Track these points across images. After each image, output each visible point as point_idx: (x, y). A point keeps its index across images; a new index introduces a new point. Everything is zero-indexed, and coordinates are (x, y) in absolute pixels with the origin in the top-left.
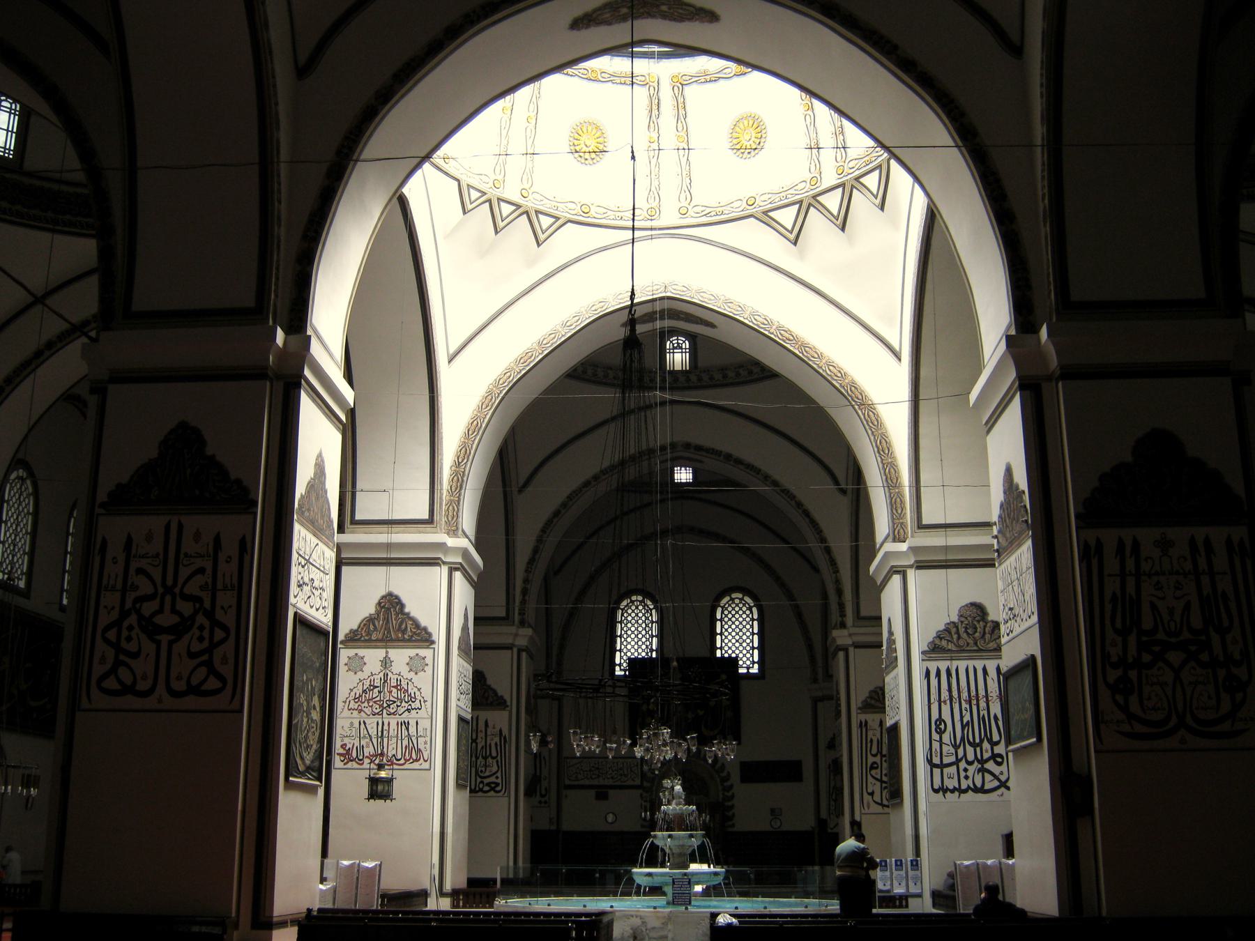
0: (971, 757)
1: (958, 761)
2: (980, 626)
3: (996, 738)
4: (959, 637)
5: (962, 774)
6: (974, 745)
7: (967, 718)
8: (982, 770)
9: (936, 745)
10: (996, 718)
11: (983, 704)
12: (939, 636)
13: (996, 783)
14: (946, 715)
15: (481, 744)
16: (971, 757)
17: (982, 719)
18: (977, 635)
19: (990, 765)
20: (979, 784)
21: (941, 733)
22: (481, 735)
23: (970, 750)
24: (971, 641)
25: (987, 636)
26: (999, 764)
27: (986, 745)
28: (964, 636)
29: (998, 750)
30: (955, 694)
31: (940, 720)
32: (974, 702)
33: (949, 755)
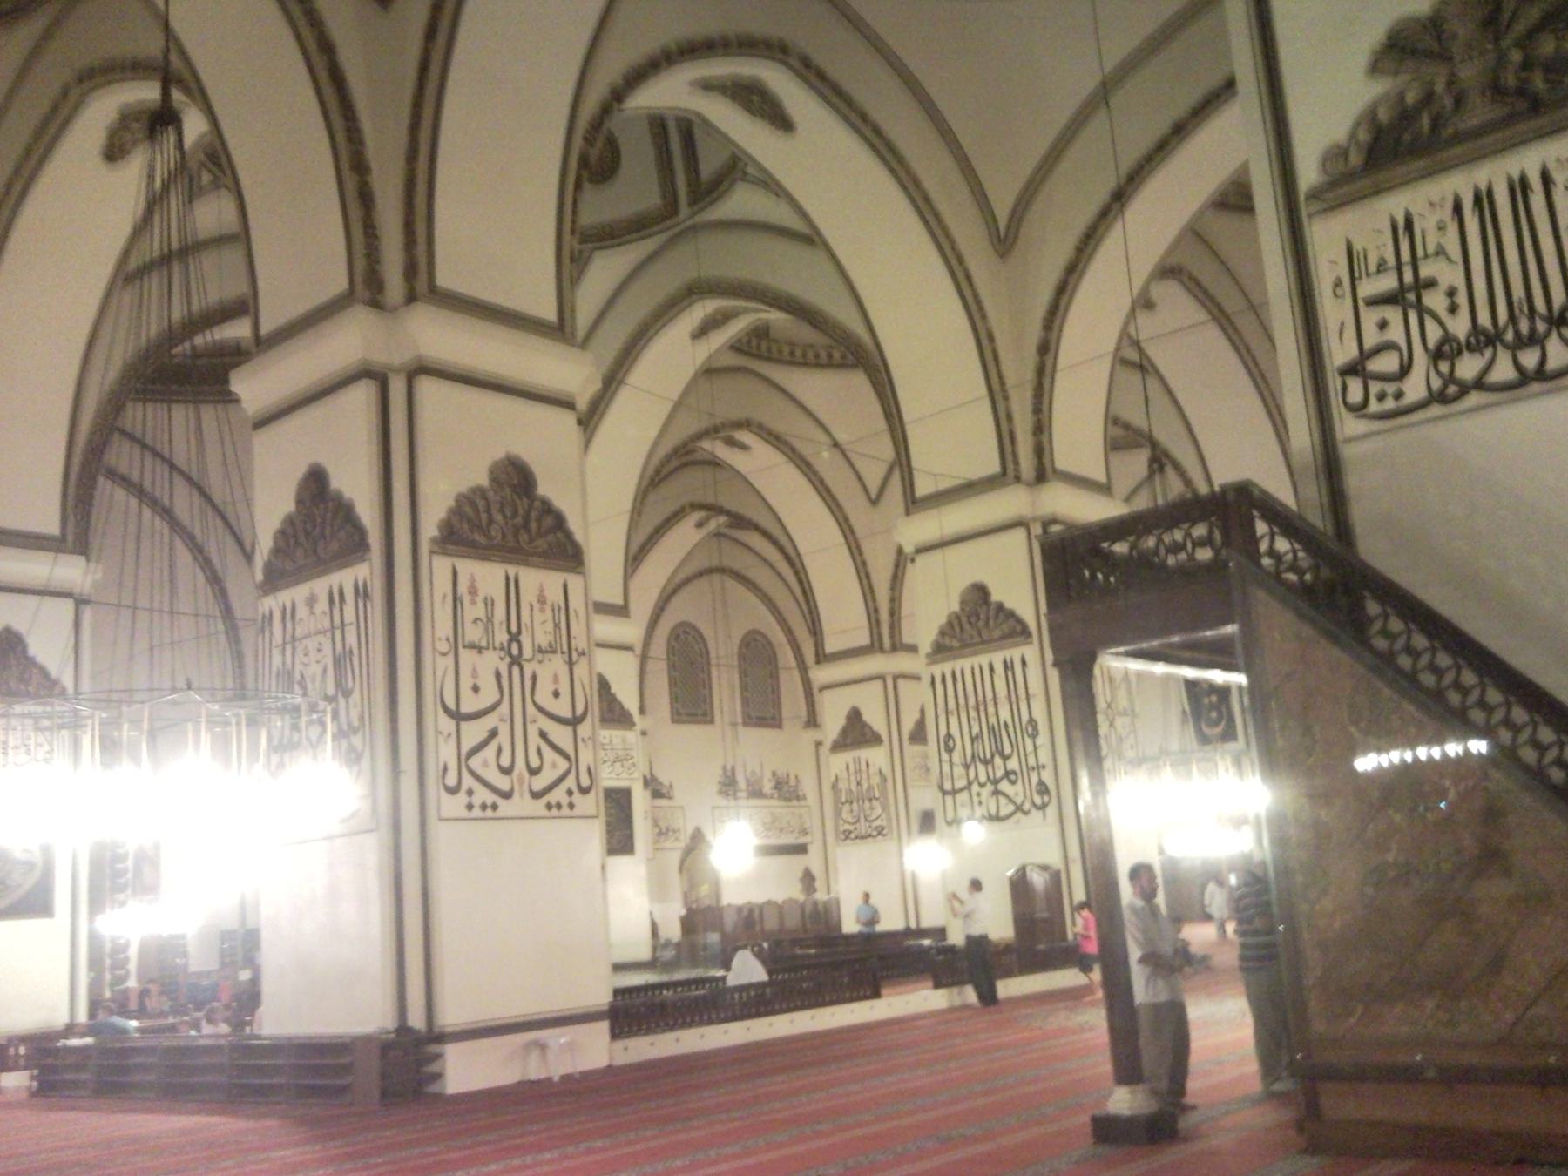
0: (983, 778)
1: (970, 783)
2: (982, 611)
3: (1007, 750)
4: (962, 629)
5: (976, 799)
6: (986, 762)
7: (976, 730)
8: (996, 793)
9: (946, 768)
10: (1006, 725)
11: (991, 709)
12: (942, 633)
13: (1011, 808)
14: (955, 731)
15: (865, 785)
16: (983, 778)
17: (991, 729)
18: (981, 624)
19: (1004, 786)
20: (993, 811)
21: (950, 751)
22: (864, 776)
23: (981, 768)
24: (974, 633)
25: (992, 623)
26: (1013, 783)
27: (998, 761)
28: (967, 626)
29: (1013, 764)
30: (962, 701)
31: (949, 736)
32: (982, 708)
33: (961, 777)
